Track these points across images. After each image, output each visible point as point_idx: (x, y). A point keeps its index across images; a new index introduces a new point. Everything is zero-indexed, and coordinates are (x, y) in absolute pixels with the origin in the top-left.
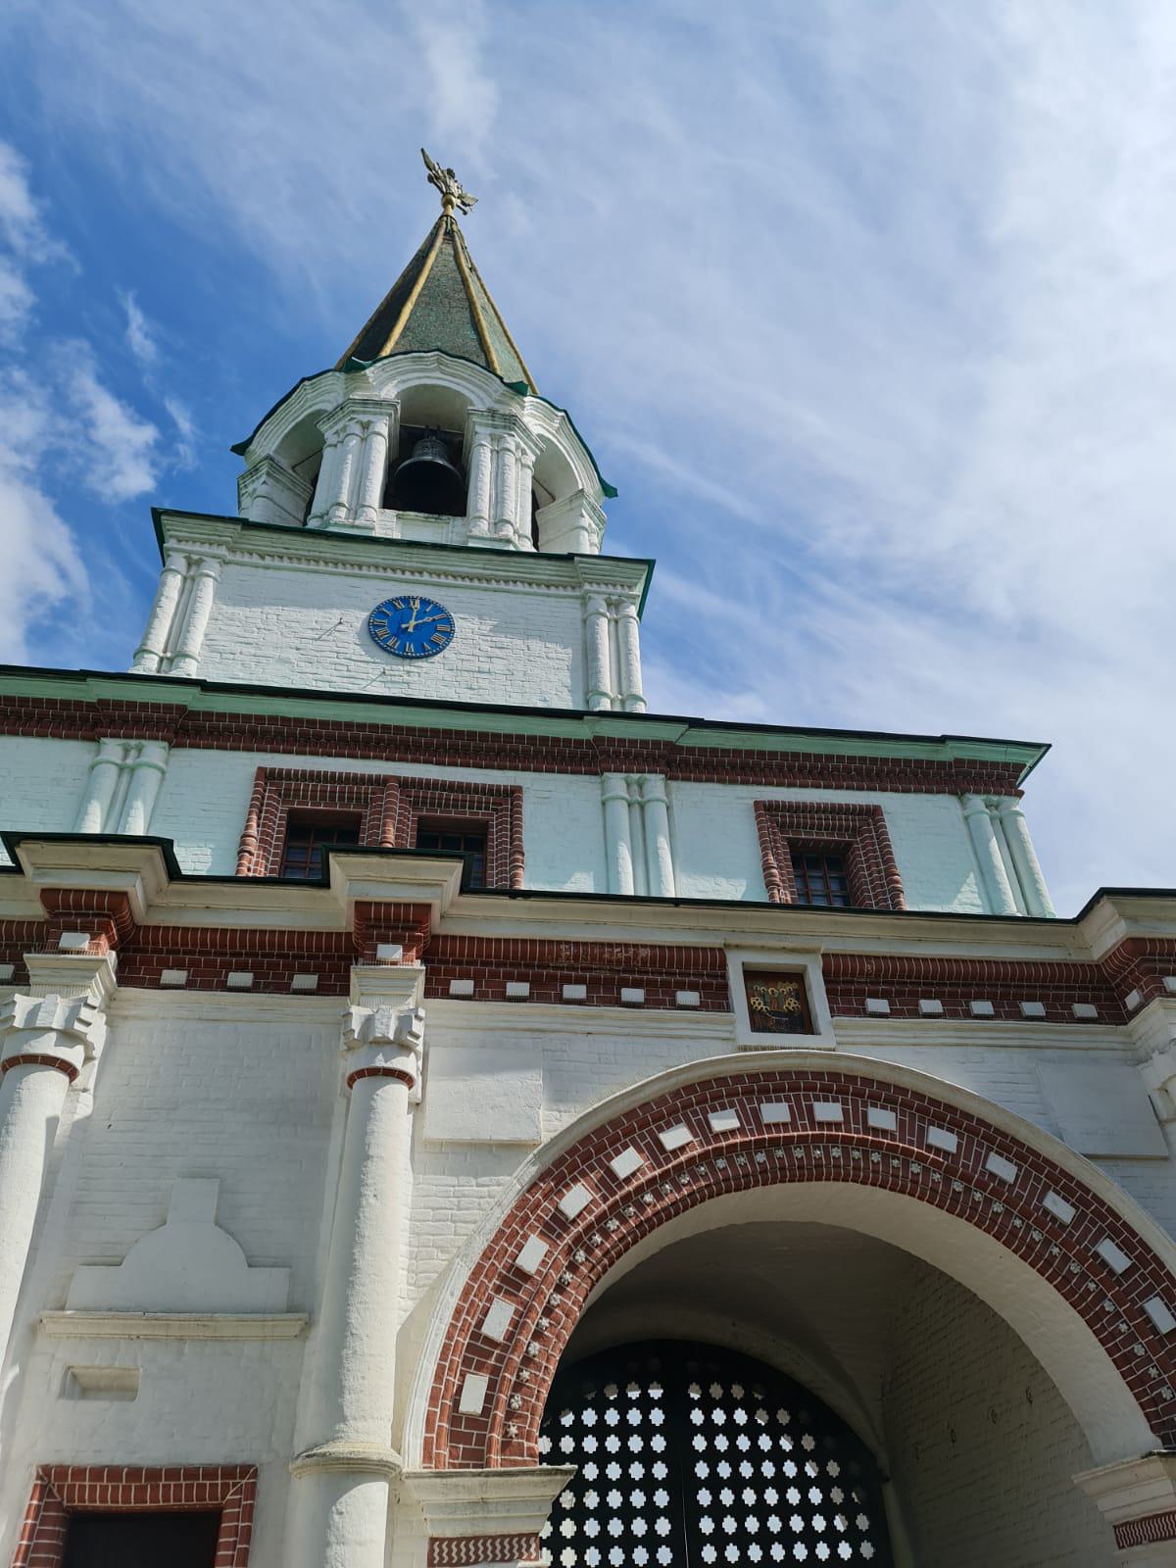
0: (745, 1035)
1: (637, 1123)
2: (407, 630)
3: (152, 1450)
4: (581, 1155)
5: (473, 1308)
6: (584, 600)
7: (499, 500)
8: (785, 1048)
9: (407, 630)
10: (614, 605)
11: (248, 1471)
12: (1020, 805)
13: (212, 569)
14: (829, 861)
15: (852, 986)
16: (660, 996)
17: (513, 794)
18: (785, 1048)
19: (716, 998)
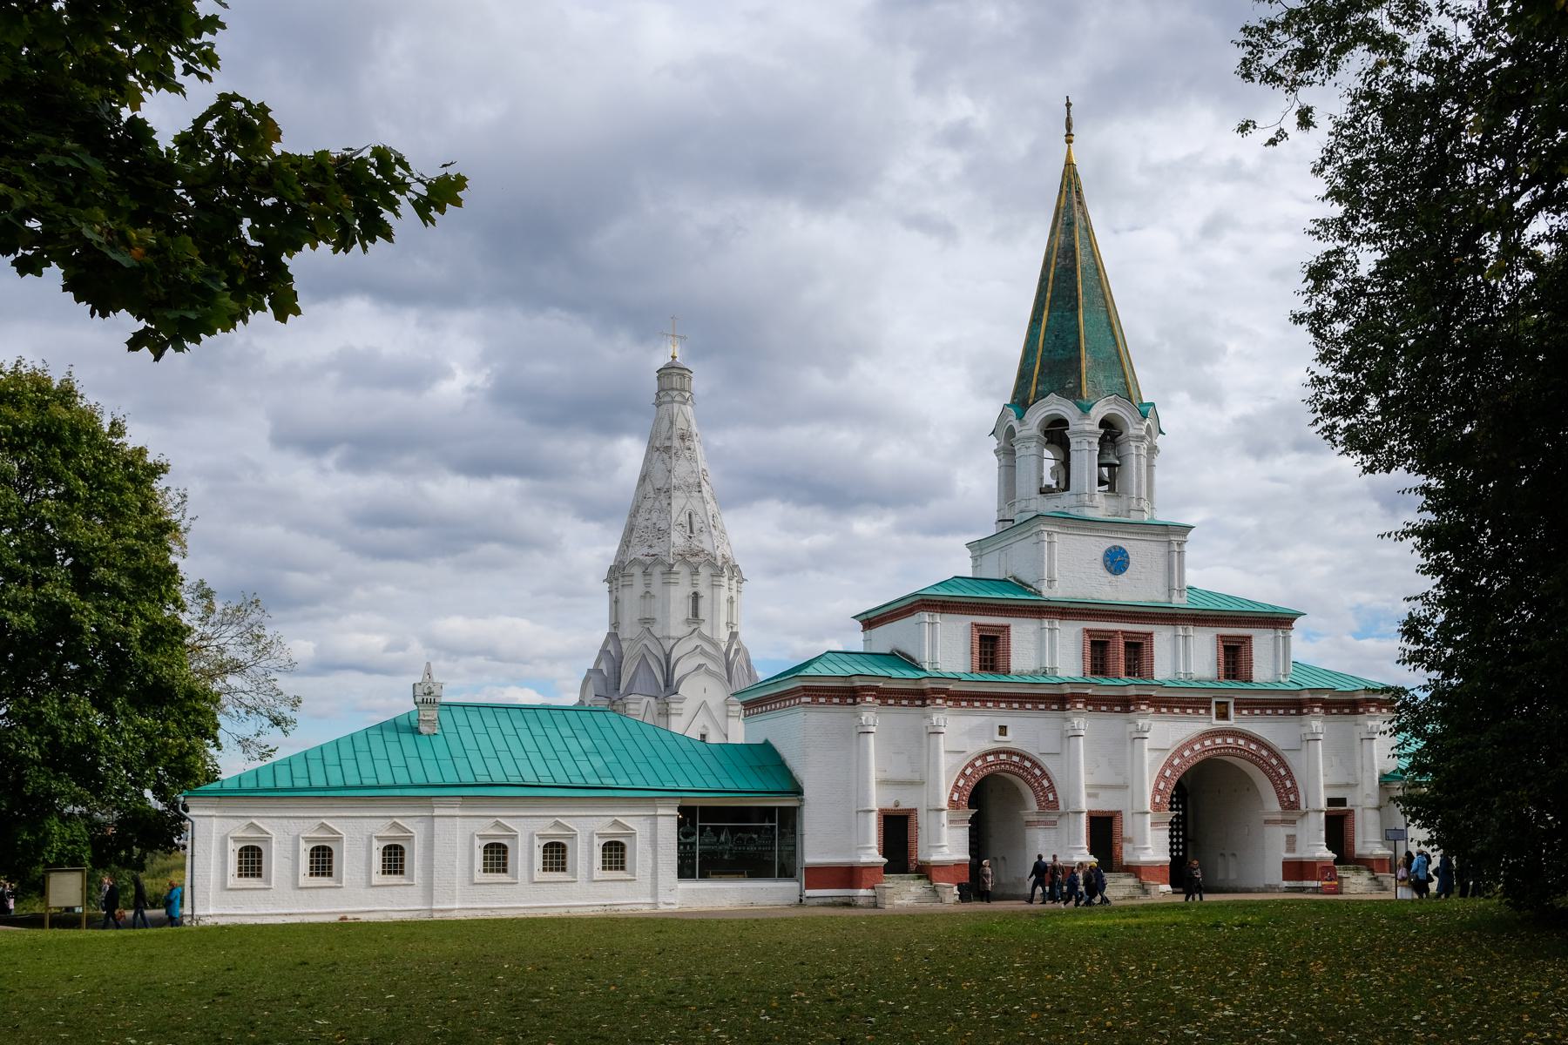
0: (1215, 721)
1: (1189, 744)
2: (1116, 562)
3: (1106, 808)
4: (1179, 752)
5: (1157, 784)
6: (1170, 542)
7: (1139, 486)
8: (1223, 724)
9: (1116, 562)
10: (1179, 545)
11: (1119, 812)
12: (1292, 633)
13: (1055, 537)
14: (1234, 657)
15: (1241, 705)
16: (1196, 710)
17: (1150, 634)
18: (1223, 724)
19: (1208, 710)
